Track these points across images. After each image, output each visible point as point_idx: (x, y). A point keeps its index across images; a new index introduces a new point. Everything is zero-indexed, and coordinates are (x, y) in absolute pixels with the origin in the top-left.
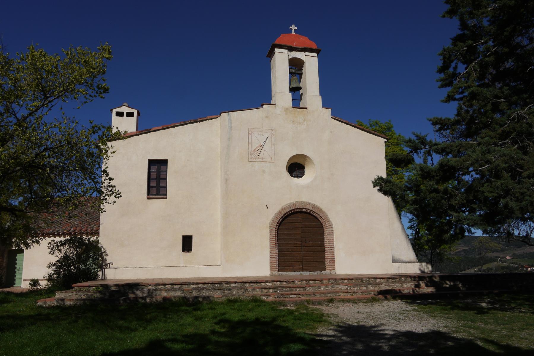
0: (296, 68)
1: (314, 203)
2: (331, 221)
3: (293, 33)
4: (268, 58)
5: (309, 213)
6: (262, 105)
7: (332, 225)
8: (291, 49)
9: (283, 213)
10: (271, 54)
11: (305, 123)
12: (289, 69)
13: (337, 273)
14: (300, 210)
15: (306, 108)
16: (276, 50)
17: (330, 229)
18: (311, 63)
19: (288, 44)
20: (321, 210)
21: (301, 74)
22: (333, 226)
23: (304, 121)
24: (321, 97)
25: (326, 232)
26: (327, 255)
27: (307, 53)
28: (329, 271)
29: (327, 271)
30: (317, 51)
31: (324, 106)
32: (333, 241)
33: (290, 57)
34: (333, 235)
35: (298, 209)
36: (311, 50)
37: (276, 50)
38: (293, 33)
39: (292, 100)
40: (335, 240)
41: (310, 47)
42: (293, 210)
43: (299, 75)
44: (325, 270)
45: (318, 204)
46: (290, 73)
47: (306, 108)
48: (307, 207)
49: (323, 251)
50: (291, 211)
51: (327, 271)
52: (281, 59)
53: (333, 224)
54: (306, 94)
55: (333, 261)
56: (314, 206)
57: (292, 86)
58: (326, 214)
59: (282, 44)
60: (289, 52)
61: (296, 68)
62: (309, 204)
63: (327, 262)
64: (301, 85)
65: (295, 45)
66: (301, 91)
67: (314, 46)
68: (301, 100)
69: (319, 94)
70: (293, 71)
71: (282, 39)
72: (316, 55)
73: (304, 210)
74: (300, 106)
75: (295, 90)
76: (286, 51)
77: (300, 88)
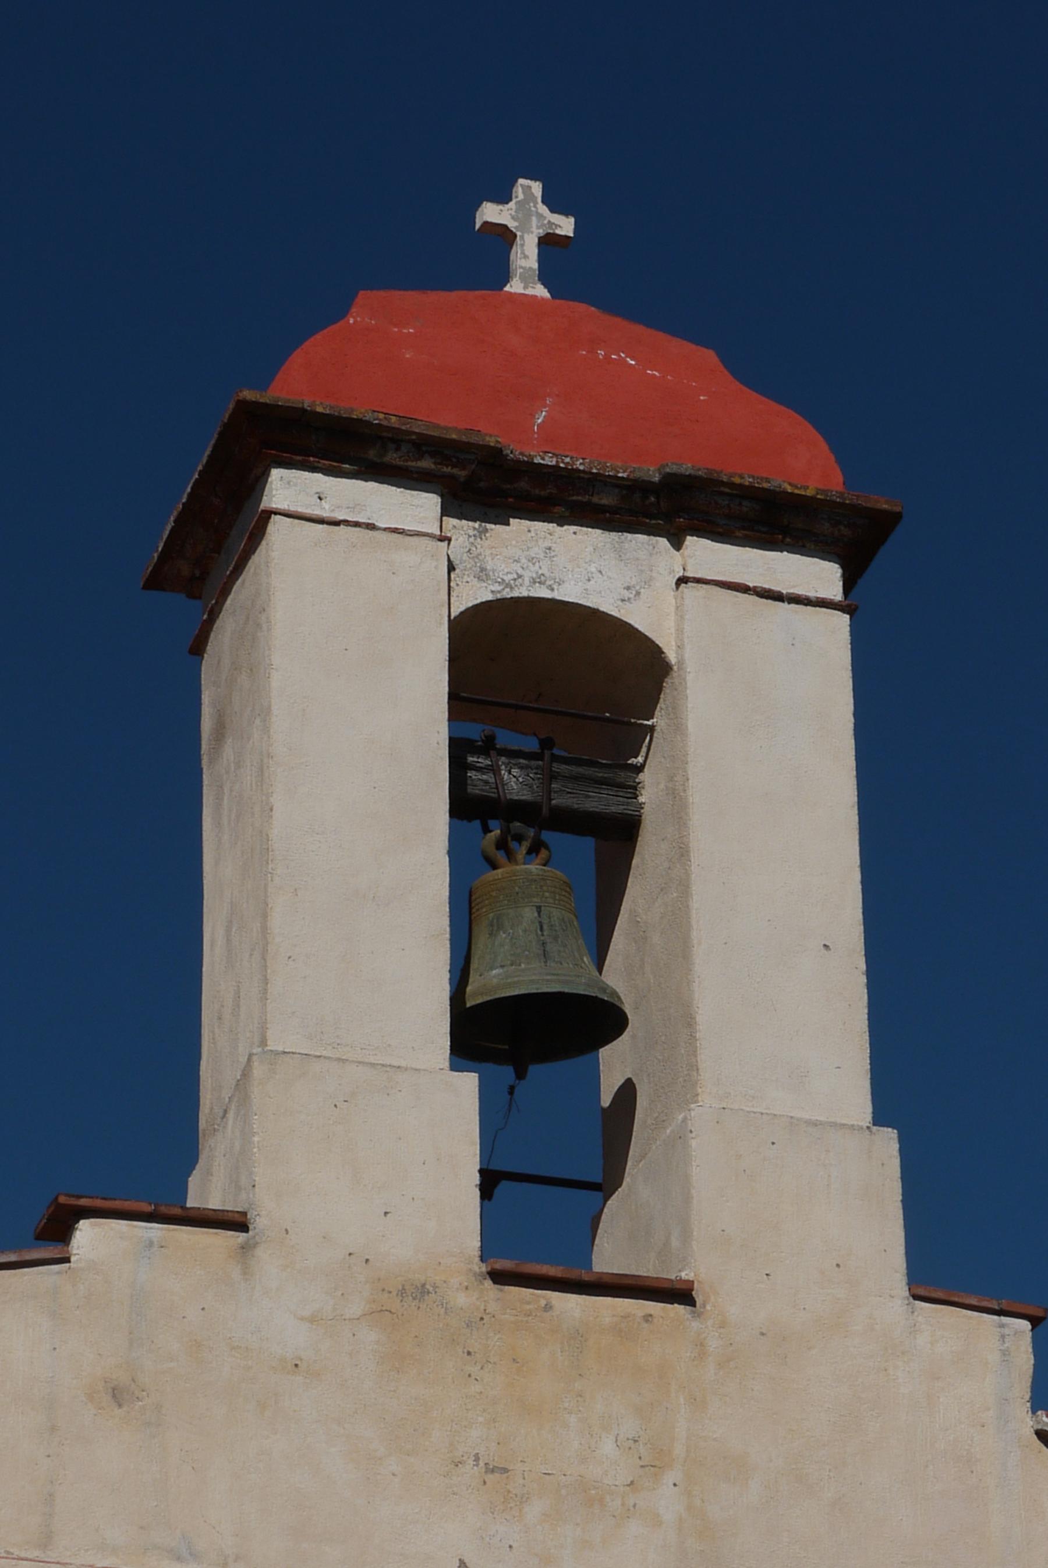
0: (549, 745)
3: (524, 278)
4: (174, 601)
6: (57, 1229)
8: (485, 485)
10: (210, 543)
11: (666, 1499)
12: (460, 753)
15: (680, 1294)
16: (286, 488)
18: (761, 689)
19: (447, 419)
21: (619, 834)
23: (656, 1465)
24: (888, 1140)
27: (705, 554)
30: (853, 537)
31: (944, 1265)
33: (472, 594)
36: (768, 519)
37: (286, 488)
38: (524, 278)
39: (490, 1181)
41: (745, 470)
43: (582, 848)
46: (466, 806)
47: (680, 1294)
52: (349, 618)
54: (689, 1094)
57: (496, 979)
59: (362, 405)
60: (461, 529)
61: (549, 745)
64: (617, 977)
65: (537, 433)
66: (615, 1063)
67: (806, 464)
68: (606, 1184)
69: (856, 1099)
70: (515, 782)
71: (376, 350)
72: (823, 577)
74: (609, 1256)
75: (538, 1045)
76: (422, 508)
77: (602, 1020)
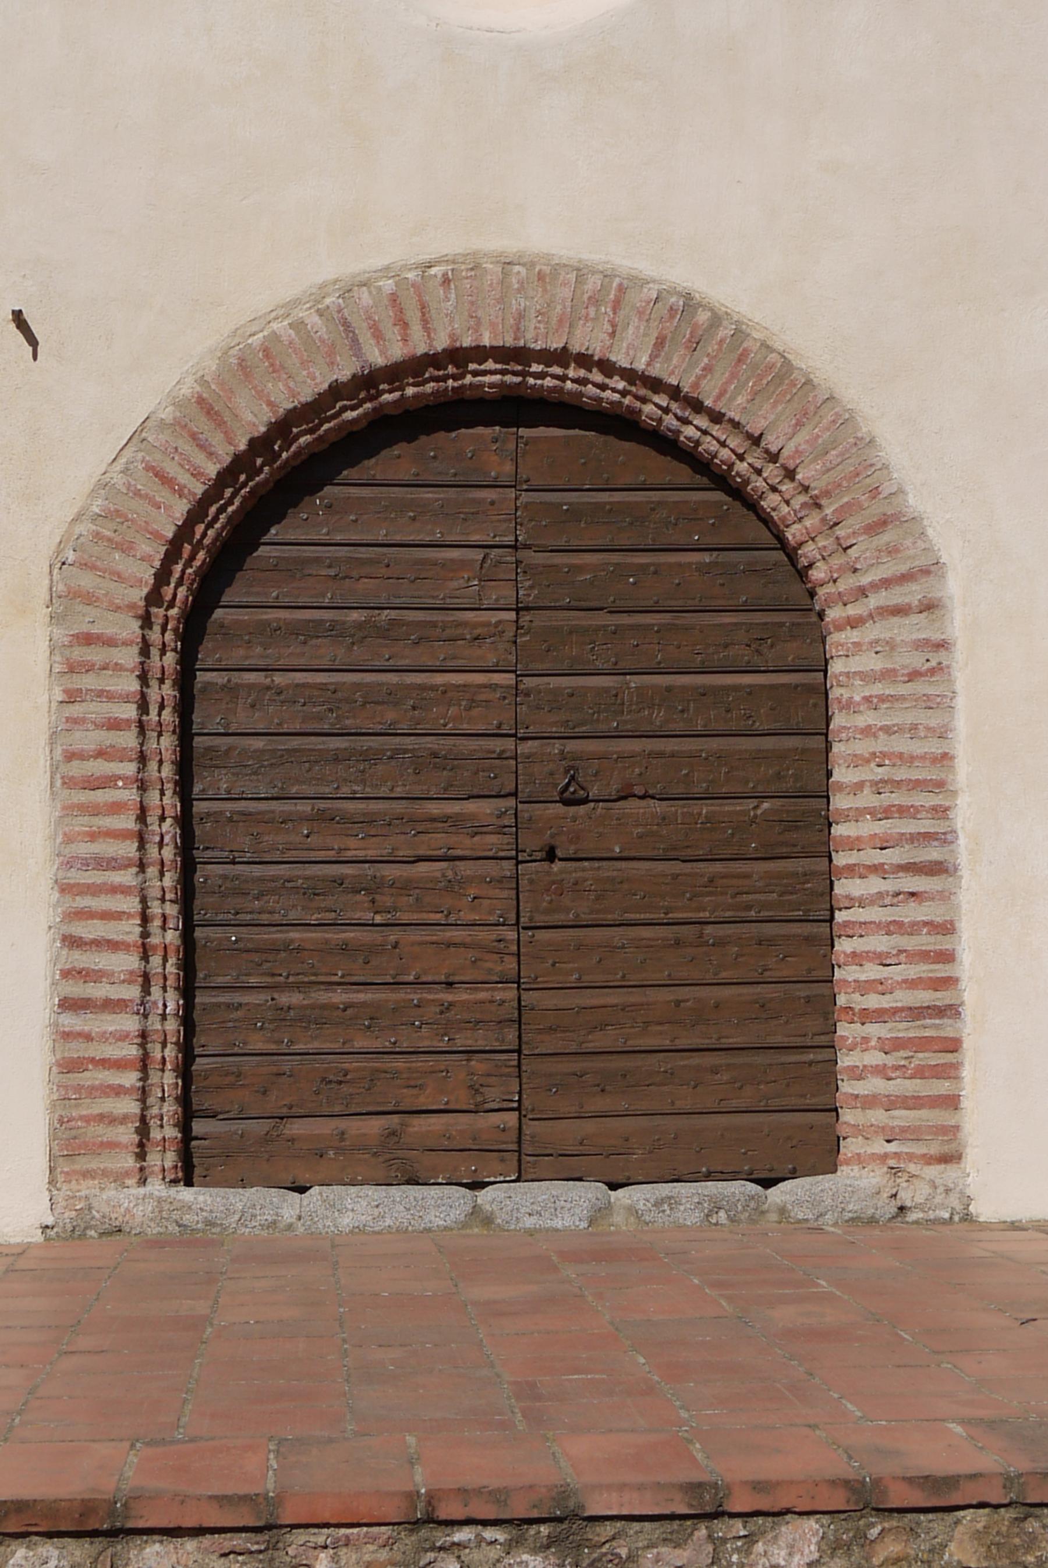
1: (680, 274)
2: (913, 524)
5: (620, 424)
7: (931, 570)
9: (253, 418)
13: (985, 1210)
14: (489, 378)
17: (907, 630)
20: (781, 377)
22: (954, 586)
25: (855, 660)
26: (864, 966)
28: (872, 1178)
29: (856, 1182)
32: (931, 781)
34: (940, 704)
35: (458, 356)
40: (963, 771)
42: (396, 373)
44: (824, 1156)
45: (740, 287)
48: (589, 339)
49: (813, 915)
50: (367, 382)
51: (846, 1174)
53: (950, 549)
55: (933, 1040)
56: (685, 317)
58: (846, 421)
62: (616, 293)
63: (861, 1054)
73: (545, 380)
